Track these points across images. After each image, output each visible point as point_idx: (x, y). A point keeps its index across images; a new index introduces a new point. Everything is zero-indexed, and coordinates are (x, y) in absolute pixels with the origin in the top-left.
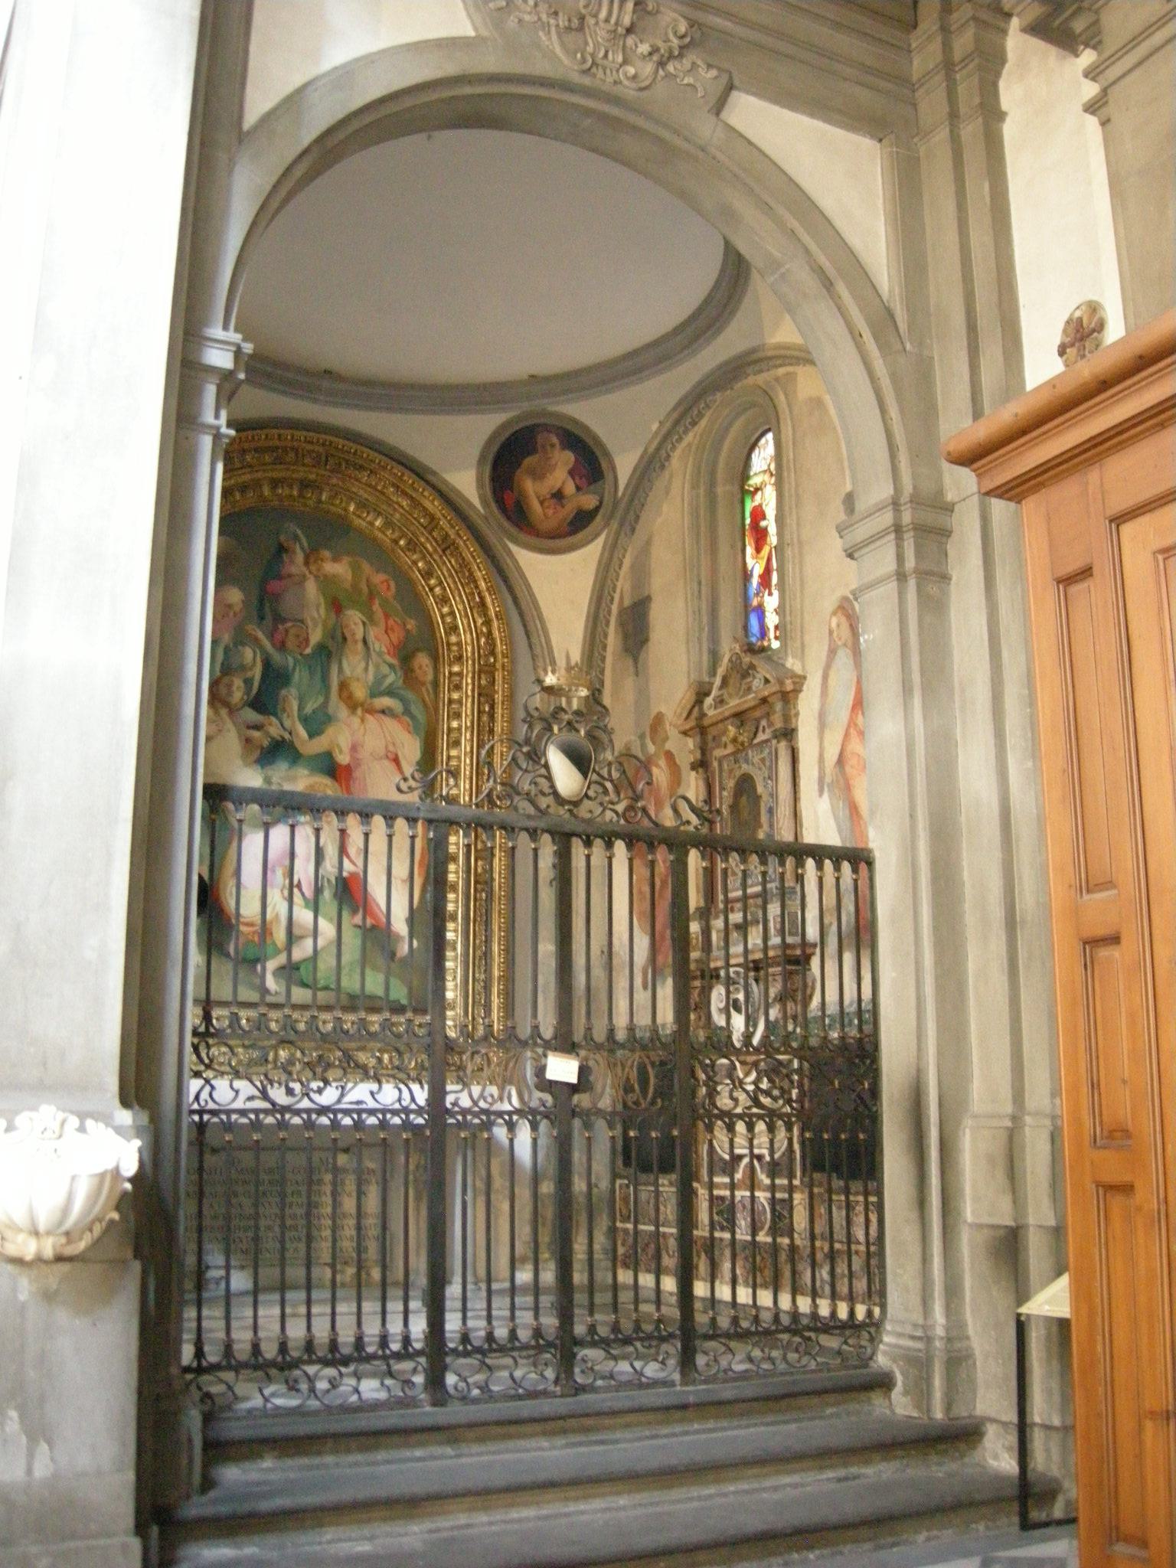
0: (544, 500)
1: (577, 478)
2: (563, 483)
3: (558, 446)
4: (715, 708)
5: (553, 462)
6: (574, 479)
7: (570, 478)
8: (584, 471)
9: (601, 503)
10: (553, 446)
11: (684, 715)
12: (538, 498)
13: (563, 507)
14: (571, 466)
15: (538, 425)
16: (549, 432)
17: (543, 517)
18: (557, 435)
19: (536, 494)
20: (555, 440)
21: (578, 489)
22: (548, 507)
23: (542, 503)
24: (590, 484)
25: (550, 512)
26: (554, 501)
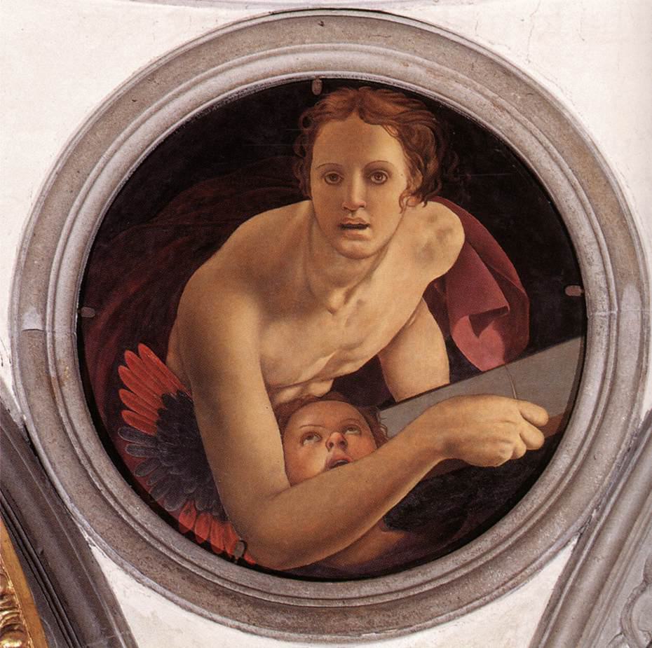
0: (304, 402)
2: (396, 341)
5: (368, 242)
6: (445, 324)
7: (429, 319)
8: (498, 299)
9: (555, 436)
10: (377, 175)
12: (272, 390)
13: (380, 439)
14: (441, 268)
15: (332, 85)
16: (370, 115)
17: (281, 478)
18: (404, 139)
19: (267, 368)
21: (460, 368)
23: (284, 416)
24: (514, 353)
25: (320, 457)
26: (343, 411)
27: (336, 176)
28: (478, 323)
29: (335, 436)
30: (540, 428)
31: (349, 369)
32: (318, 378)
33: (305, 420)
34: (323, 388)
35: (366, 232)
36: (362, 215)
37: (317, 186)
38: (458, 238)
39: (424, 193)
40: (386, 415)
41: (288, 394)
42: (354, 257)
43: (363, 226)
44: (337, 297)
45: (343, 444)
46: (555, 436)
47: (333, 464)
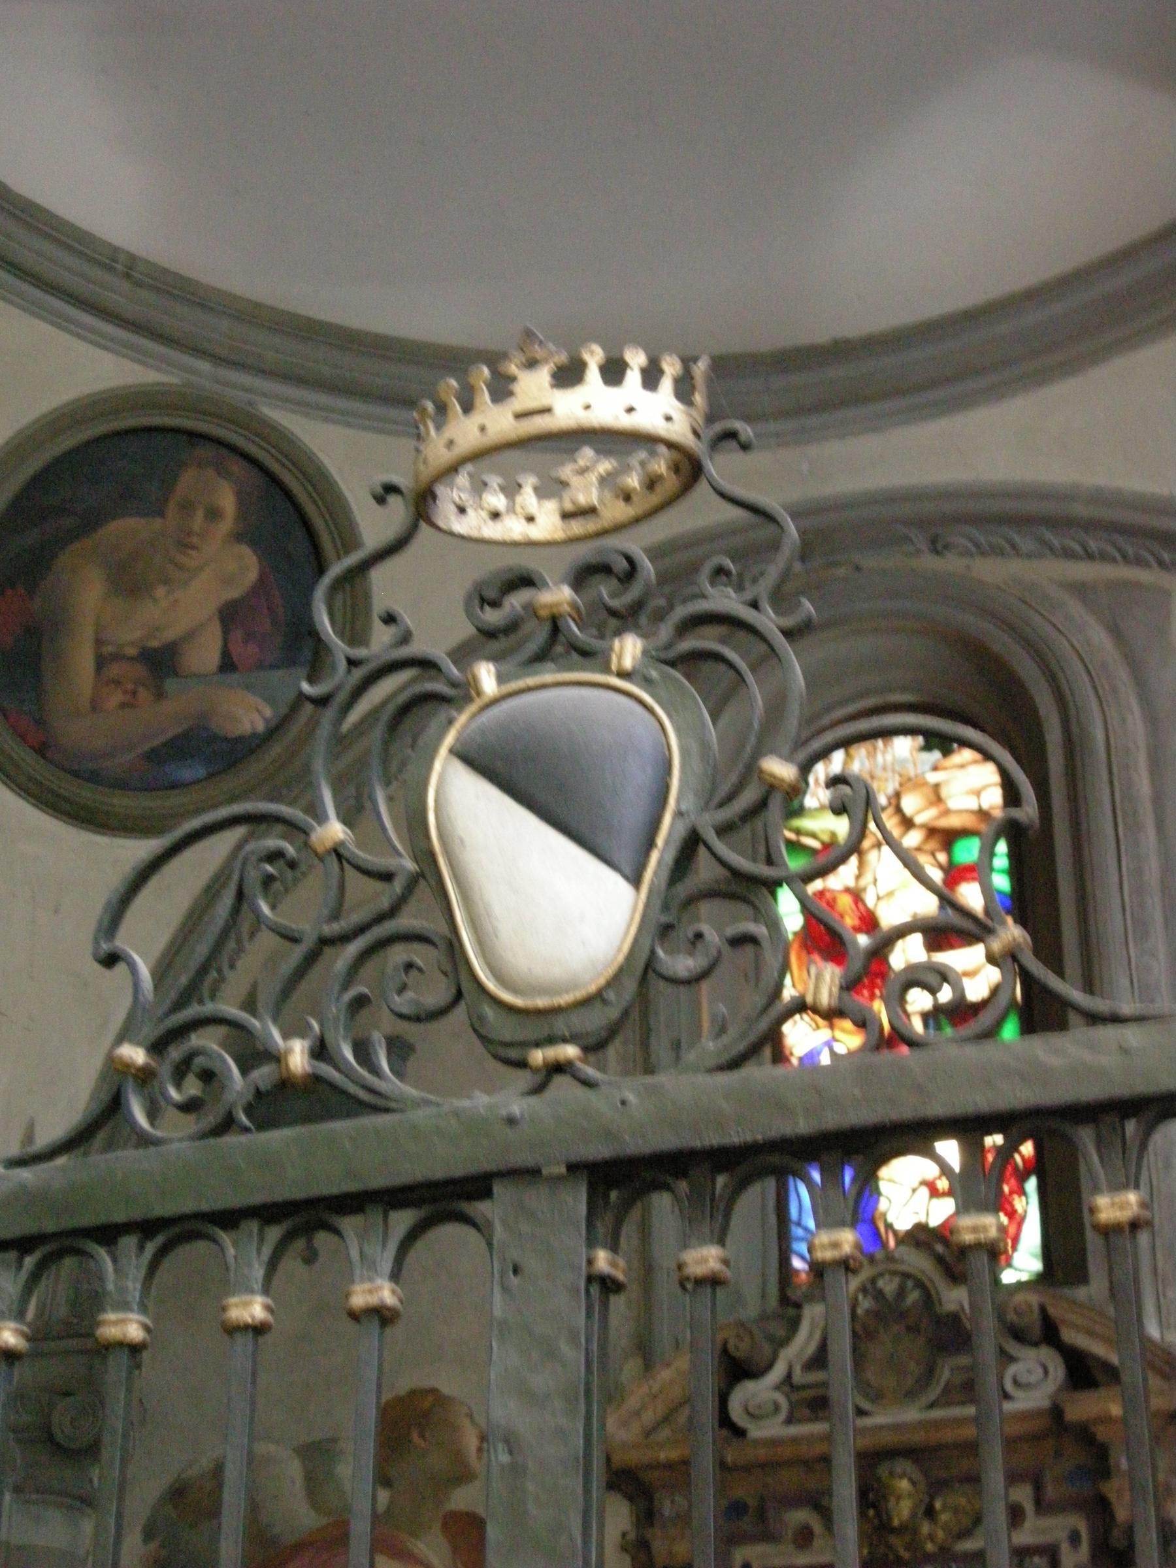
0: (117, 657)
1: (238, 634)
3: (227, 524)
4: (789, 1421)
6: (226, 632)
10: (214, 514)
11: (649, 1417)
12: (99, 642)
13: (160, 695)
14: (234, 593)
16: (222, 471)
18: (238, 494)
20: (227, 501)
21: (228, 665)
22: (117, 683)
23: (101, 662)
25: (115, 698)
26: (140, 670)
27: (187, 507)
28: (249, 637)
29: (130, 686)
30: (265, 719)
31: (154, 644)
32: (132, 644)
33: (115, 670)
34: (132, 651)
35: (194, 553)
36: (195, 540)
37: (172, 508)
38: (252, 575)
39: (238, 537)
40: (170, 684)
41: (110, 649)
42: (180, 567)
43: (194, 547)
44: (160, 591)
45: (134, 693)
46: (275, 731)
47: (123, 705)
